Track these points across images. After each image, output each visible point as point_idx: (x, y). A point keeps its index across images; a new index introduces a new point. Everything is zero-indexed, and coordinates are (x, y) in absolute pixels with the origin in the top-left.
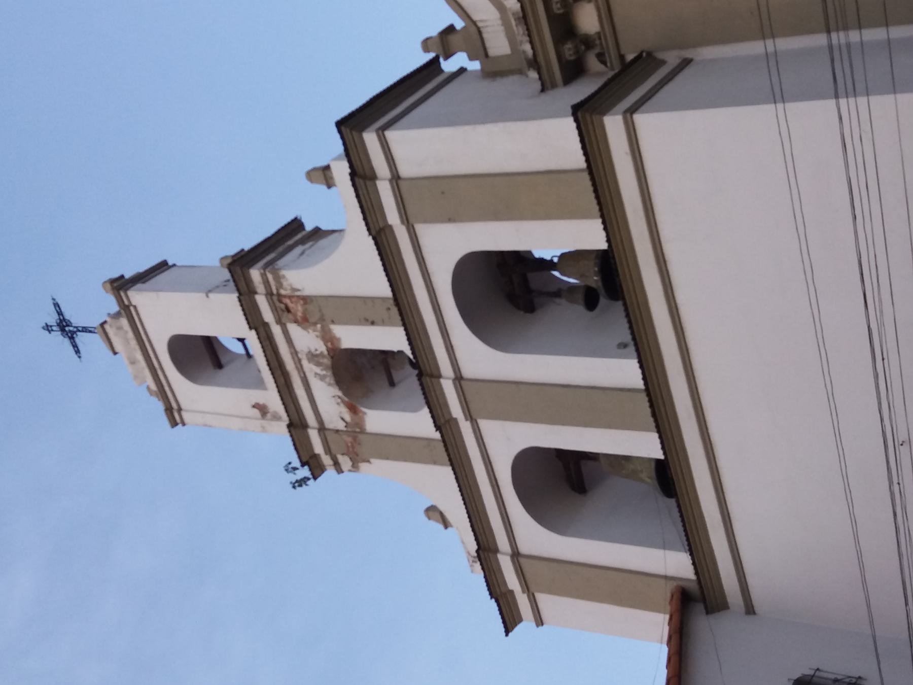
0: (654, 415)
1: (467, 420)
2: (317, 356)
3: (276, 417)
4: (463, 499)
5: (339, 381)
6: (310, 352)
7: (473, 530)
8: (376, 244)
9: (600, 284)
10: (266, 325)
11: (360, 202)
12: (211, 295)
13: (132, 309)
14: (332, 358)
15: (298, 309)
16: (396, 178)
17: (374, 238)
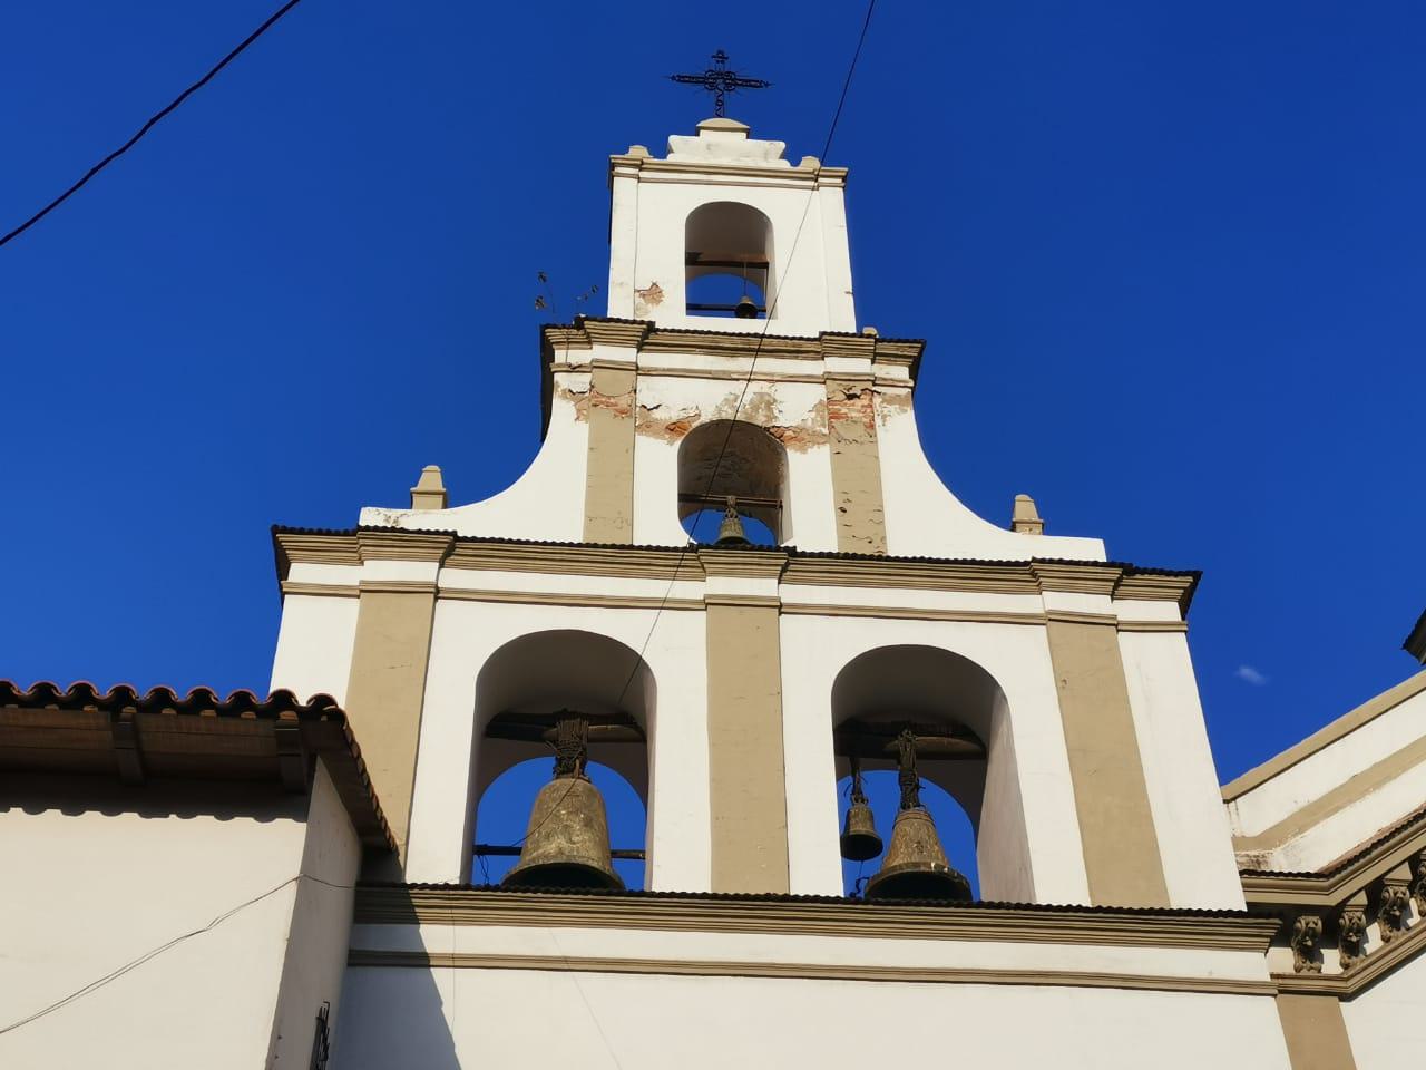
0: (768, 897)
1: (706, 597)
2: (770, 410)
3: (636, 309)
4: (553, 544)
5: (719, 425)
6: (775, 401)
7: (492, 540)
8: (1017, 564)
9: (923, 869)
10: (821, 356)
11: (1086, 564)
12: (851, 298)
13: (812, 183)
14: (767, 429)
15: (854, 409)
16: (1118, 626)
17: (1026, 563)
